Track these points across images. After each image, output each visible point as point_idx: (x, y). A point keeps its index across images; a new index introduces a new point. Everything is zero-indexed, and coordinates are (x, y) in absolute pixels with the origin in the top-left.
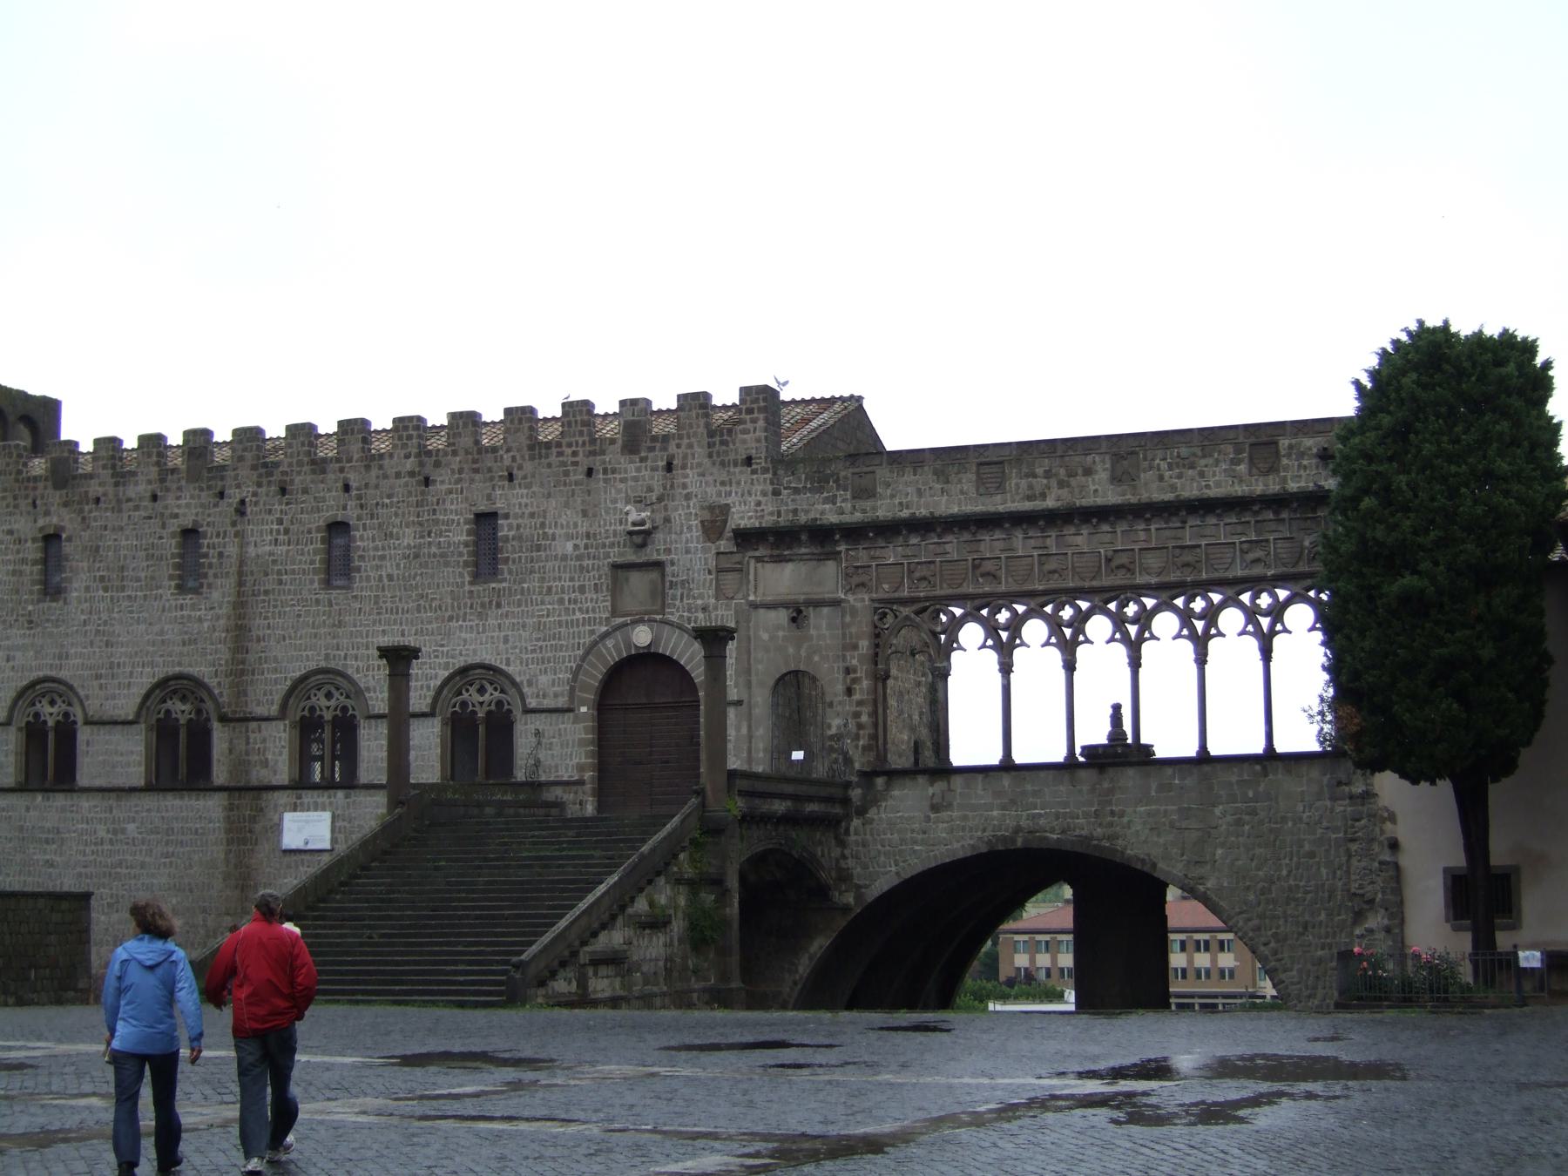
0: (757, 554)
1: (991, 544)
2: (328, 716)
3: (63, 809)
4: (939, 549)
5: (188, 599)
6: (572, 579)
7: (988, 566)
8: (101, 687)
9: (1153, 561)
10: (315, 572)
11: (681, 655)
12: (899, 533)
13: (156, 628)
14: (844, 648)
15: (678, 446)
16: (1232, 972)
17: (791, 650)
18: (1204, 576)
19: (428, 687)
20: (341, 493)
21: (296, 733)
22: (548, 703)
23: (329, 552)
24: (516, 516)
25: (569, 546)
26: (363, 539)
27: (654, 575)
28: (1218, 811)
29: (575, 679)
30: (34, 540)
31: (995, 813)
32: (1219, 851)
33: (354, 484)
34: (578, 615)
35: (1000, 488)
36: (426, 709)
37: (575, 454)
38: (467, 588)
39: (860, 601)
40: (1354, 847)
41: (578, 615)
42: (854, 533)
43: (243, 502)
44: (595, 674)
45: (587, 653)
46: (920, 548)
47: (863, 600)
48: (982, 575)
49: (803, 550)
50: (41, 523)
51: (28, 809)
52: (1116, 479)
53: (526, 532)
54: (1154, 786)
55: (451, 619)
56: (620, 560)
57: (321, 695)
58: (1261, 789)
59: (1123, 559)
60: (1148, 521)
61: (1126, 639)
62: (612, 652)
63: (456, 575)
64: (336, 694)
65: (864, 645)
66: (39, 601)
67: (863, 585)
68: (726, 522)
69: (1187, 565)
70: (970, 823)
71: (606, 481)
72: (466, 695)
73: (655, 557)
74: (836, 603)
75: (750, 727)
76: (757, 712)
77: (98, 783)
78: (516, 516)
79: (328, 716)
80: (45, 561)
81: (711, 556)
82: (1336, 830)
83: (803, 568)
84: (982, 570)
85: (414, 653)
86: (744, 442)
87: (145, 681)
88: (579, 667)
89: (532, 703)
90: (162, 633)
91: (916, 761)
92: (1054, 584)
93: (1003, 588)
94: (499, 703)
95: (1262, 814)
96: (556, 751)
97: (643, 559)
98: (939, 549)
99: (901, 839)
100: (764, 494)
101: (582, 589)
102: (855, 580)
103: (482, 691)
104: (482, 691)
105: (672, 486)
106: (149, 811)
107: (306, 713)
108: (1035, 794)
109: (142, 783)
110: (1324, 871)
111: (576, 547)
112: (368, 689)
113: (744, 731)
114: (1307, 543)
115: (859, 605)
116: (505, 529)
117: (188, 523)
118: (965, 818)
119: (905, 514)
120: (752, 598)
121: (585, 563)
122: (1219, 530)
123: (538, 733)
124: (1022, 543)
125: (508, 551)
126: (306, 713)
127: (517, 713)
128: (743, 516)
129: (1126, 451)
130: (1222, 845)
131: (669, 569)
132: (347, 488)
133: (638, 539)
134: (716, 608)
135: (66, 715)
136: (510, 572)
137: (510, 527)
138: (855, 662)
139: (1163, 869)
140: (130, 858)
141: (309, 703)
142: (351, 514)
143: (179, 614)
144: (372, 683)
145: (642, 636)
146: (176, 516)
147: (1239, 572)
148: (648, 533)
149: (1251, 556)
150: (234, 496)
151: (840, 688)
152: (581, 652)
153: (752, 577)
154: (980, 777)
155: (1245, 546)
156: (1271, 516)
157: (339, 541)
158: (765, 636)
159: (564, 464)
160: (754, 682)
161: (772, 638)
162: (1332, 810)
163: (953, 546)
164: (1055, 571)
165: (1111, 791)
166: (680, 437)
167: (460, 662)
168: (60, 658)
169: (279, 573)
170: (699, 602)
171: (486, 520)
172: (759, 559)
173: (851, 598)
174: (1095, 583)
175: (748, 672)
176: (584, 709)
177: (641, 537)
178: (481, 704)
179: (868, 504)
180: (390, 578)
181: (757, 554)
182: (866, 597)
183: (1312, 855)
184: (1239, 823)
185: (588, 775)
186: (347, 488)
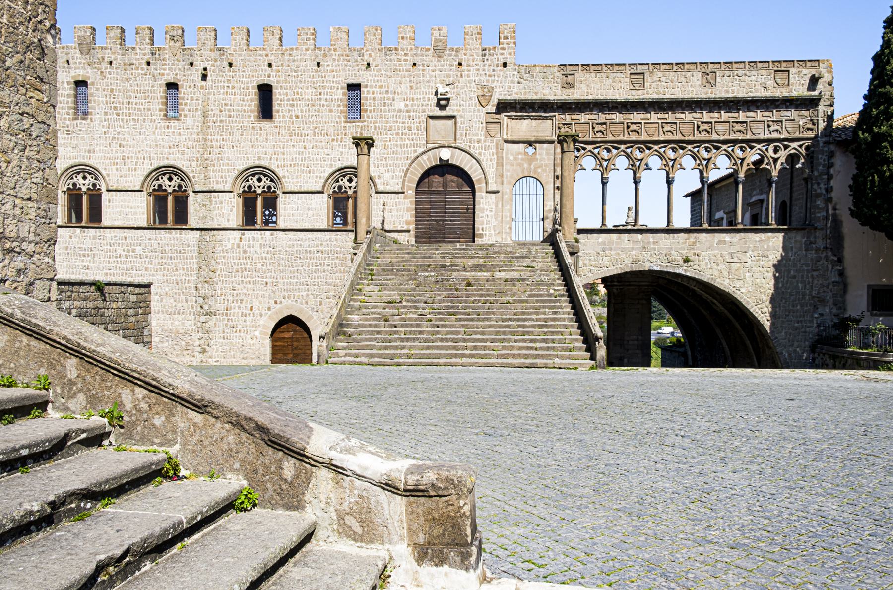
3: (95, 238)
6: (403, 123)
7: (633, 127)
8: (117, 169)
9: (721, 128)
10: (251, 111)
11: (465, 165)
13: (153, 138)
15: (465, 54)
17: (526, 165)
18: (748, 137)
19: (320, 177)
20: (267, 68)
22: (389, 188)
24: (371, 87)
26: (278, 96)
27: (450, 122)
28: (748, 255)
29: (405, 176)
30: (68, 83)
31: (634, 252)
33: (274, 64)
34: (407, 142)
36: (320, 189)
37: (406, 54)
38: (343, 124)
40: (815, 274)
41: (407, 142)
43: (205, 69)
45: (413, 162)
50: (73, 73)
51: (71, 237)
53: (377, 96)
54: (716, 241)
55: (333, 140)
56: (431, 114)
57: (255, 179)
58: (771, 244)
59: (706, 126)
62: (428, 161)
66: (74, 119)
68: (491, 96)
69: (740, 131)
71: (423, 70)
72: (341, 182)
78: (371, 87)
81: (483, 114)
83: (534, 122)
86: (502, 54)
88: (408, 169)
89: (381, 188)
90: (156, 141)
91: (603, 224)
93: (642, 138)
96: (395, 213)
100: (513, 82)
101: (410, 129)
105: (461, 76)
106: (150, 239)
108: (654, 243)
109: (145, 225)
111: (406, 105)
112: (284, 177)
113: (500, 206)
114: (801, 123)
120: (505, 137)
121: (412, 114)
124: (653, 116)
125: (367, 104)
131: (459, 120)
132: (270, 65)
133: (442, 102)
134: (485, 142)
135: (94, 185)
136: (368, 117)
137: (368, 92)
140: (138, 265)
141: (247, 184)
142: (272, 81)
143: (167, 130)
144: (286, 174)
145: (445, 154)
146: (163, 75)
147: (767, 136)
148: (448, 100)
149: (772, 128)
150: (200, 65)
152: (409, 161)
153: (505, 126)
155: (771, 123)
158: (512, 158)
159: (399, 60)
160: (505, 182)
161: (516, 159)
162: (806, 256)
164: (670, 131)
165: (695, 243)
166: (466, 49)
167: (339, 165)
168: (89, 152)
169: (229, 110)
170: (476, 138)
172: (510, 117)
174: (691, 138)
175: (502, 176)
176: (410, 192)
178: (350, 187)
179: (571, 90)
180: (297, 117)
183: (794, 277)
185: (412, 227)
186: (270, 65)
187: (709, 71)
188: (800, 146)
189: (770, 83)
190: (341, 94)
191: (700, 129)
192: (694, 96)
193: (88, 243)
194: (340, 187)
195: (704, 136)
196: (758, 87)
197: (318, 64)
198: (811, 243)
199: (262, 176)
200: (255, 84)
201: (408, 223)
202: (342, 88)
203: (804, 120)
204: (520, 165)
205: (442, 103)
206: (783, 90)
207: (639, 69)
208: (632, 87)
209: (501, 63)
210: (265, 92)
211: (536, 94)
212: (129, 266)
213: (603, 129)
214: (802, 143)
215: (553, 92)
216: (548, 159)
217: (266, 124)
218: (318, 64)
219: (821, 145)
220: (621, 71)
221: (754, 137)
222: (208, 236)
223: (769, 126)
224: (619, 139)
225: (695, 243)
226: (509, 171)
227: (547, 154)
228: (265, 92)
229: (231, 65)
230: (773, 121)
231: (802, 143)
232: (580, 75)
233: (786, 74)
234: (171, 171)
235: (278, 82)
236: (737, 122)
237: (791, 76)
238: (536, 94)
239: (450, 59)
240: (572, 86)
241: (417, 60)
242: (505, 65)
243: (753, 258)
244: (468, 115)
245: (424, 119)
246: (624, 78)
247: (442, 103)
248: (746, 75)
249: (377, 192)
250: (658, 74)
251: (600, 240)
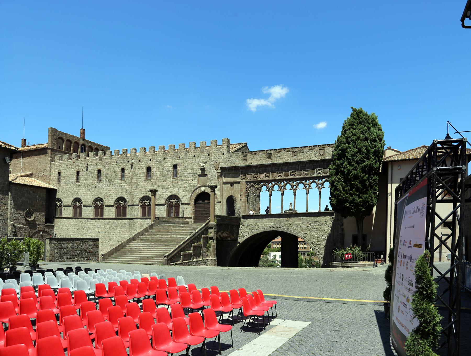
5: (123, 182)
14: (241, 191)
22: (186, 202)
25: (190, 171)
39: (243, 182)
60: (299, 165)
62: (198, 192)
63: (170, 176)
65: (244, 191)
76: (224, 203)
77: (108, 217)
80: (98, 175)
81: (216, 173)
85: (156, 191)
87: (115, 197)
89: (183, 202)
99: (248, 230)
116: (179, 168)
117: (122, 167)
119: (253, 164)
123: (184, 208)
128: (223, 165)
132: (150, 160)
139: (297, 235)
142: (151, 165)
145: (203, 189)
149: (318, 172)
150: (131, 162)
151: (239, 199)
161: (227, 189)
167: (170, 194)
171: (175, 167)
185: (193, 216)
187: (294, 150)
189: (317, 154)
190: (171, 169)
193: (99, 224)
196: (313, 156)
197: (165, 158)
204: (228, 191)
205: (203, 170)
207: (269, 152)
210: (149, 169)
212: (110, 231)
217: (149, 181)
218: (165, 158)
220: (263, 153)
222: (131, 221)
223: (317, 171)
227: (238, 187)
228: (149, 169)
229: (139, 161)
234: (121, 199)
239: (205, 154)
241: (195, 154)
242: (224, 154)
244: (211, 173)
245: (197, 176)
246: (265, 156)
247: (203, 170)
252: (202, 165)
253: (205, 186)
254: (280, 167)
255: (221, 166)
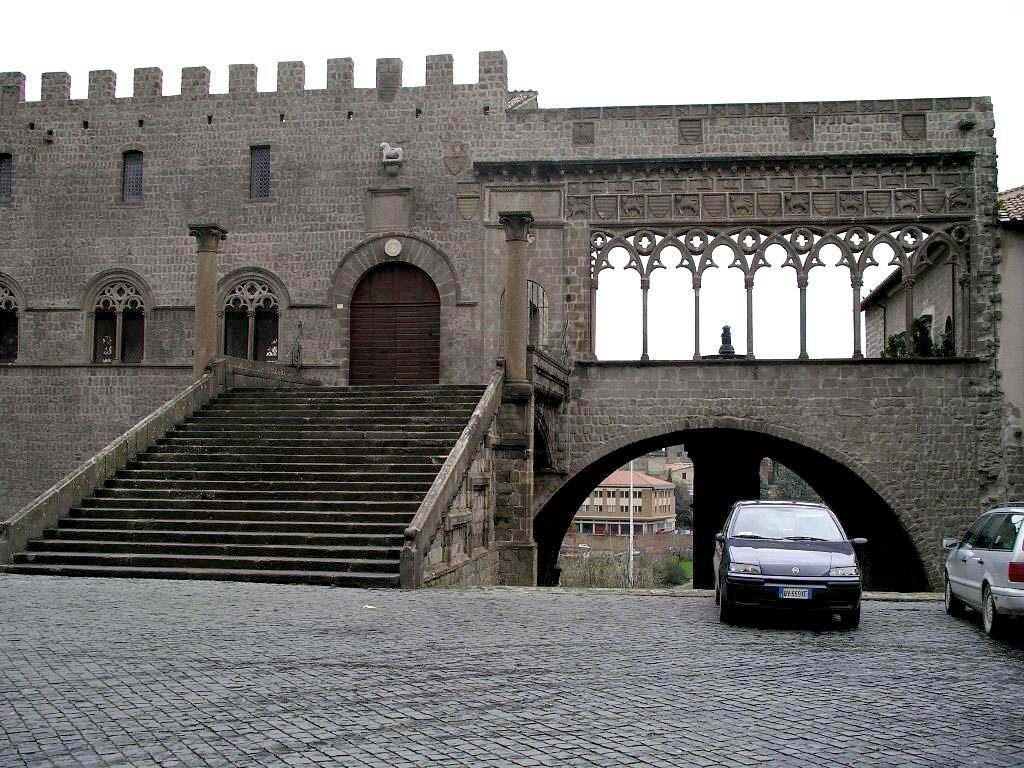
0: (492, 184)
1: (690, 184)
2: (119, 308)
4: (646, 186)
7: (687, 201)
9: (824, 203)
12: (614, 171)
14: (566, 262)
16: (640, 507)
18: (865, 216)
20: (137, 128)
21: (92, 321)
23: (124, 174)
28: (873, 402)
32: (874, 435)
35: (698, 139)
39: (580, 225)
40: (982, 434)
42: (576, 169)
43: (50, 133)
44: (351, 278)
46: (633, 184)
47: (582, 224)
48: (683, 208)
49: (532, 183)
52: (793, 137)
54: (822, 381)
57: (114, 291)
58: (908, 386)
59: (799, 200)
60: (820, 171)
61: (797, 266)
62: (365, 261)
64: (127, 291)
67: (582, 212)
69: (852, 207)
70: (669, 407)
73: (404, 185)
74: (559, 226)
75: (483, 323)
79: (119, 308)
82: (967, 420)
84: (682, 204)
92: (742, 217)
93: (699, 219)
94: (267, 301)
95: (910, 406)
97: (394, 186)
98: (646, 186)
102: (576, 208)
103: (252, 290)
104: (252, 290)
107: (101, 306)
110: (957, 452)
112: (155, 287)
115: (579, 228)
116: (276, 160)
118: (665, 402)
122: (879, 181)
124: (716, 184)
126: (101, 306)
127: (282, 308)
129: (801, 115)
130: (876, 430)
133: (390, 169)
138: (574, 274)
145: (393, 248)
148: (399, 164)
149: (903, 202)
153: (486, 203)
154: (678, 370)
155: (899, 194)
156: (920, 172)
157: (132, 166)
160: (486, 289)
163: (659, 184)
164: (743, 208)
165: (787, 384)
172: (493, 189)
173: (571, 222)
177: (391, 168)
178: (252, 300)
181: (492, 184)
182: (585, 222)
183: (947, 439)
184: (890, 412)
185: (343, 361)
188: (949, 231)
189: (897, 133)
190: (239, 161)
191: (791, 204)
192: (779, 154)
194: (237, 301)
195: (796, 216)
198: (971, 383)
199: (125, 287)
200: (118, 151)
201: (335, 354)
202: (243, 152)
203: (952, 191)
206: (918, 144)
208: (682, 141)
209: (480, 108)
211: (535, 152)
213: (637, 205)
214: (950, 225)
215: (559, 149)
216: (555, 253)
219: (980, 228)
221: (874, 216)
223: (897, 199)
224: (663, 220)
225: (787, 384)
226: (493, 272)
229: (86, 125)
230: (903, 191)
231: (950, 225)
232: (600, 126)
233: (919, 121)
235: (151, 147)
236: (847, 193)
237: (928, 123)
238: (535, 152)
240: (590, 140)
243: (882, 409)
246: (671, 127)
248: (858, 122)
249: (292, 307)
250: (721, 123)
251: (637, 380)
252: (388, 150)
253: (399, 236)
254: (743, 177)
255: (475, 158)
